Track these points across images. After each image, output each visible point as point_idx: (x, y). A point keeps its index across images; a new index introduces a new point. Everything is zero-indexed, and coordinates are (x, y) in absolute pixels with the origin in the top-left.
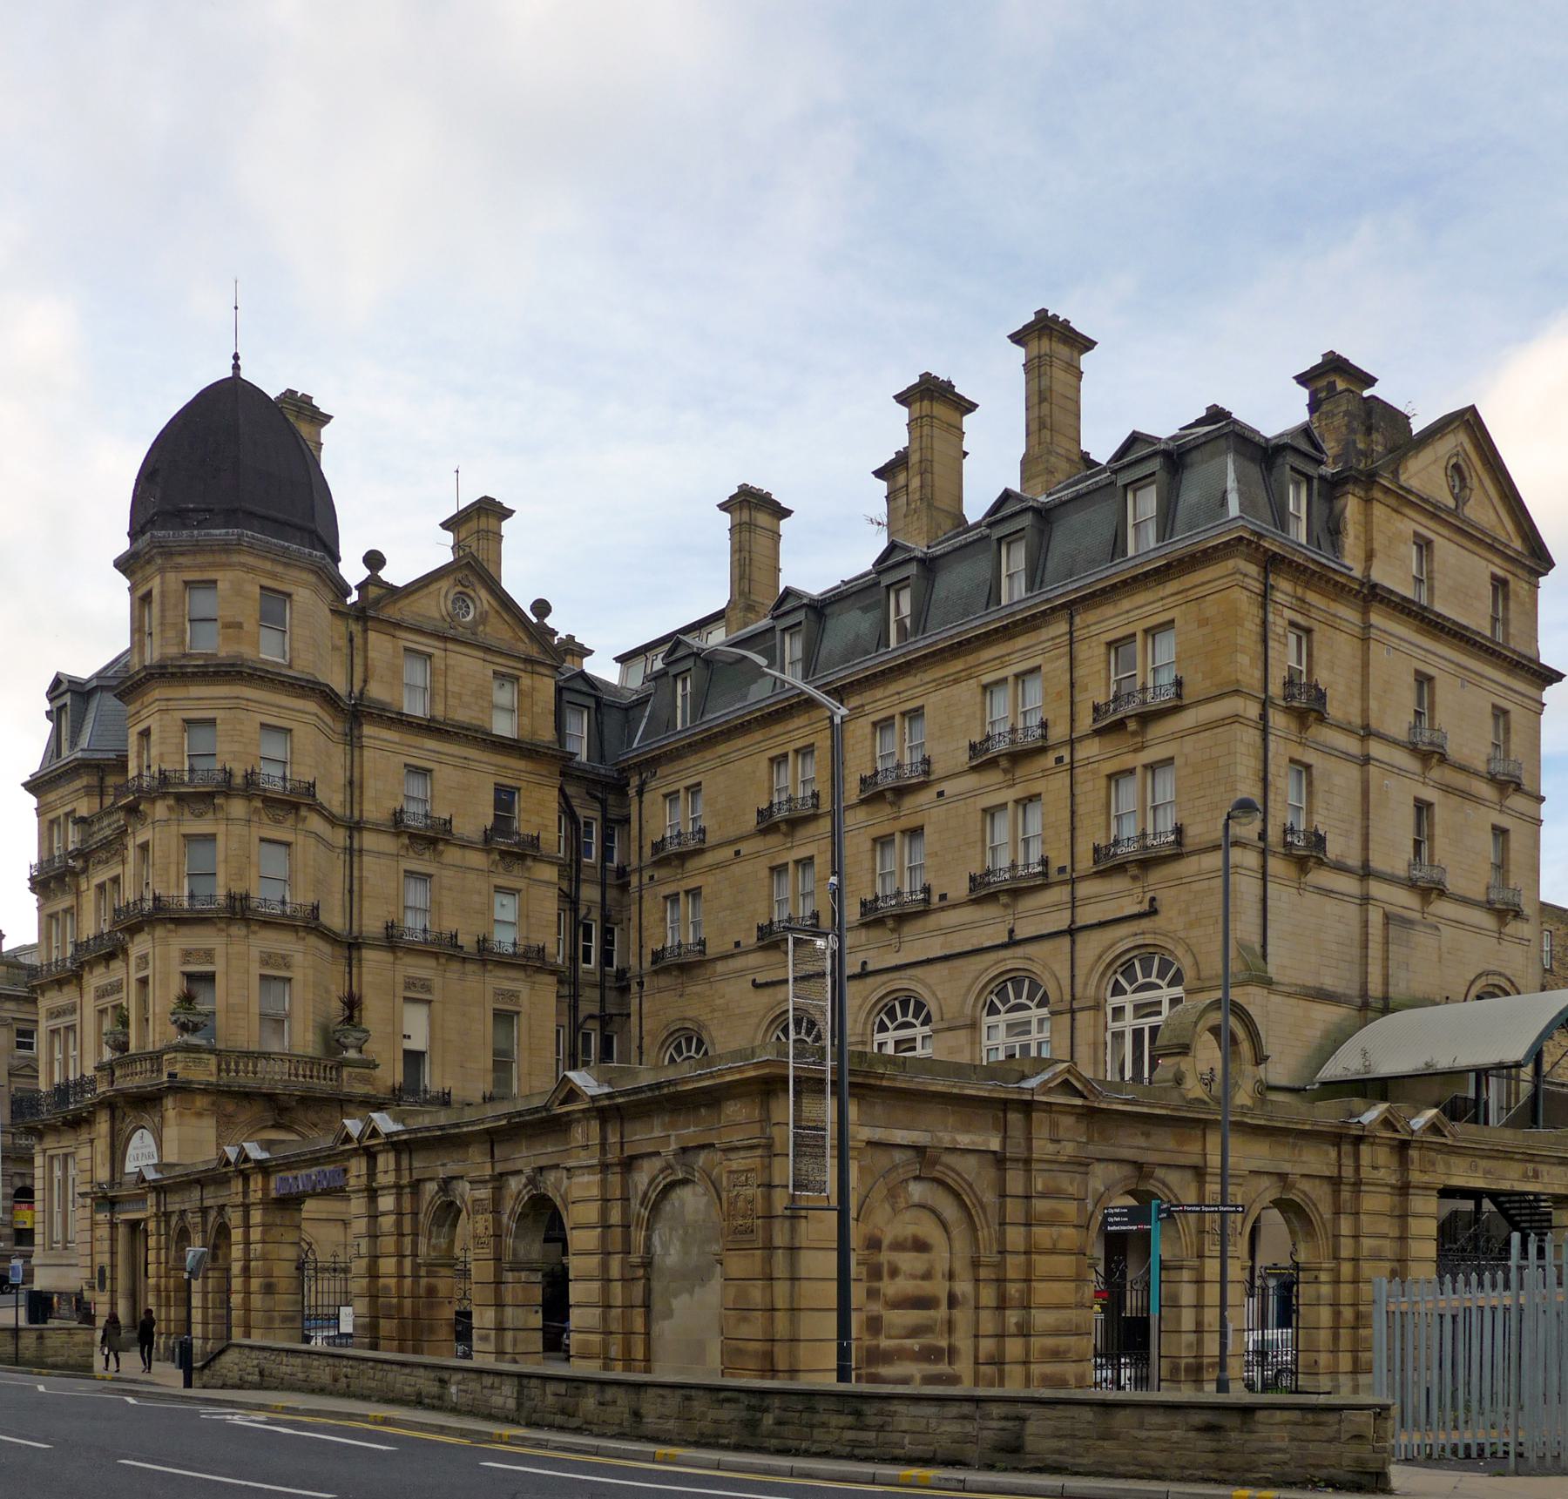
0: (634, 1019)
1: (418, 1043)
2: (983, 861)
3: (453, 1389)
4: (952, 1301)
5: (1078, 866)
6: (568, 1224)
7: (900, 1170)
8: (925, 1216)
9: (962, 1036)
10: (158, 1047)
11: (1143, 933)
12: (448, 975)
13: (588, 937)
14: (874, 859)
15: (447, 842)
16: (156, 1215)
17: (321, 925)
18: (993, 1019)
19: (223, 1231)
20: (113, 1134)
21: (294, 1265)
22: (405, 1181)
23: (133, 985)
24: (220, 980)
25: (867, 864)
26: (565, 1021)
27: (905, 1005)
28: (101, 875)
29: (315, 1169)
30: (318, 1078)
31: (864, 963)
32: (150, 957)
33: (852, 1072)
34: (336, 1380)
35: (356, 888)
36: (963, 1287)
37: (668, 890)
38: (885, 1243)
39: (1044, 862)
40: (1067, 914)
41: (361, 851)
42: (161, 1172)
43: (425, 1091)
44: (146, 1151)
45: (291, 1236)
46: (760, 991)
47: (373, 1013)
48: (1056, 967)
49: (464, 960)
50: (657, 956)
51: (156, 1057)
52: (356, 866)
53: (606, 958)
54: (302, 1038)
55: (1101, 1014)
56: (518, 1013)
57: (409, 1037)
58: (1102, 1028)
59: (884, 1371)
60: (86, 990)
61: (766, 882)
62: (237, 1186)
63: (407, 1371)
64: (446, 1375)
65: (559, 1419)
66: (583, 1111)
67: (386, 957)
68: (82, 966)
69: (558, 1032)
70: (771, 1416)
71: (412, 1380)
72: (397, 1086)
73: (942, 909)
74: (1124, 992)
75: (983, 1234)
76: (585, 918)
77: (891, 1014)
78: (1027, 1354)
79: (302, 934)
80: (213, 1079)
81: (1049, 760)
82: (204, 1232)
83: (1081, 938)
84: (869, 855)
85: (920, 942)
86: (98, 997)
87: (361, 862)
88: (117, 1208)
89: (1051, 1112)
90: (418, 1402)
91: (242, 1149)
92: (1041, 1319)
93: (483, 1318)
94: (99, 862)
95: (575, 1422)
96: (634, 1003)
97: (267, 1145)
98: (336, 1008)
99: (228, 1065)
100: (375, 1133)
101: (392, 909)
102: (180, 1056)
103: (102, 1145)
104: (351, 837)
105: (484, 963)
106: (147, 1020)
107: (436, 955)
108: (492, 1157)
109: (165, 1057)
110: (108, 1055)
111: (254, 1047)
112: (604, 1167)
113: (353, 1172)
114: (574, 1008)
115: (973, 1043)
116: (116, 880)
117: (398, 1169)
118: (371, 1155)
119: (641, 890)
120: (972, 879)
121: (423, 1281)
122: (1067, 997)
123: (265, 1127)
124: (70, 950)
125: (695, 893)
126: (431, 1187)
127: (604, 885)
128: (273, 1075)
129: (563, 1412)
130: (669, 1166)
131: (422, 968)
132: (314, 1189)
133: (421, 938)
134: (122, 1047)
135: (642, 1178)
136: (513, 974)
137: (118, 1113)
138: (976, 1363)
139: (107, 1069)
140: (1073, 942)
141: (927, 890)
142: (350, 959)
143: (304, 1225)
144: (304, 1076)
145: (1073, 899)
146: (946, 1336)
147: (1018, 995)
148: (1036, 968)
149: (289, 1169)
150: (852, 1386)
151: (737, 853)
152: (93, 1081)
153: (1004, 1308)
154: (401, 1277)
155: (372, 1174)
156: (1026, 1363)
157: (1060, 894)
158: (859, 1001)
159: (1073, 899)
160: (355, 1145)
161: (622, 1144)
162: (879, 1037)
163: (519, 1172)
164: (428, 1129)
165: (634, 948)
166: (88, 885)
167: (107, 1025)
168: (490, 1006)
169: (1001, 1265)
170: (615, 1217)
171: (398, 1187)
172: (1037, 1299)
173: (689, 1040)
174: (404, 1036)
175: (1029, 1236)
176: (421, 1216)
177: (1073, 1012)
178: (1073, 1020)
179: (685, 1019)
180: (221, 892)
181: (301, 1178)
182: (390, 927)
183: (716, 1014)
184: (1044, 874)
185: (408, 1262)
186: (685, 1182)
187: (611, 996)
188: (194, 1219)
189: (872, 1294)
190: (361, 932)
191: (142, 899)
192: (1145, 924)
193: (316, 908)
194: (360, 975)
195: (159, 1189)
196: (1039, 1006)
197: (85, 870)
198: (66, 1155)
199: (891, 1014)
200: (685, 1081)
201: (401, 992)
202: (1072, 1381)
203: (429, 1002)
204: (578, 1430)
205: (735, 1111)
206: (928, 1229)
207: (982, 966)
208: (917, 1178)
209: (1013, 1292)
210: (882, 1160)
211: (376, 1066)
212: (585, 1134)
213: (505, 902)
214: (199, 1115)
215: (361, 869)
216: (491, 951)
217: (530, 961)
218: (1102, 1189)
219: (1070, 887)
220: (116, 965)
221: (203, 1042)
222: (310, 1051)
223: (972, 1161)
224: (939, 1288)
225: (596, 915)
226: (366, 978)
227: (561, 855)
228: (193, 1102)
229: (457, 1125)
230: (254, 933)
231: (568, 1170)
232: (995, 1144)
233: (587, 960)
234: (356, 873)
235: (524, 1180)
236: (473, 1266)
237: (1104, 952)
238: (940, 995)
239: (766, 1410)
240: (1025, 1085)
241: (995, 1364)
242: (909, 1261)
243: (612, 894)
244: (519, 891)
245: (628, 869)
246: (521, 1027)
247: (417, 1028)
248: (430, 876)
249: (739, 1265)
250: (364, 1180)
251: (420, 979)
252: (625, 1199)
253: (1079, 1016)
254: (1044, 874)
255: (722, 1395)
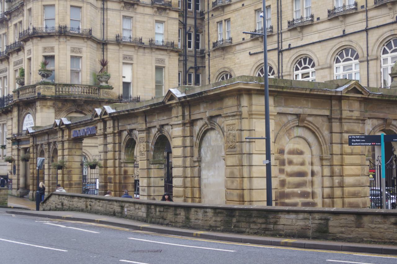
0: (207, 68)
1: (127, 80)
2: (333, 5)
3: (126, 210)
4: (313, 174)
5: (368, 5)
6: (172, 146)
7: (291, 123)
8: (301, 141)
9: (327, 71)
10: (35, 83)
11: (394, 30)
12: (139, 54)
13: (190, 38)
14: (293, 5)
15: (137, 4)
16: (33, 146)
17: (92, 37)
18: (338, 64)
19: (56, 151)
20: (19, 116)
21: (80, 163)
22: (116, 131)
23: (26, 61)
24: (56, 58)
25: (290, 8)
26: (182, 69)
27: (305, 60)
28: (16, 21)
29: (86, 127)
30: (92, 93)
31: (290, 45)
32: (32, 50)
33: (270, 86)
34: (87, 207)
35: (105, 22)
36: (317, 168)
37: (218, 19)
38: (286, 151)
39: (356, 4)
40: (365, 23)
41: (107, 9)
42: (35, 130)
43: (131, 97)
44: (30, 122)
45: (78, 152)
46: (252, 56)
47: (112, 67)
49: (144, 48)
50: (215, 44)
51: (34, 86)
52: (105, 15)
53: (197, 46)
54: (86, 78)
55: (379, 61)
56: (164, 67)
57: (125, 77)
58: (379, 67)
59: (287, 201)
60: (10, 63)
61: (254, 15)
62: (60, 134)
63: (110, 203)
64: (123, 204)
65: (161, 220)
66: (176, 103)
67: (116, 48)
68: (9, 54)
69: (179, 74)
70: (235, 219)
71: (112, 206)
72: (120, 95)
73: (318, 23)
74: (387, 53)
75: (324, 147)
76: (189, 31)
77: (300, 64)
78: (343, 194)
79: (85, 40)
80: (54, 94)
82: (49, 152)
83: (370, 33)
84: (291, 4)
85: (311, 36)
86: (15, 65)
87: (107, 13)
88: (20, 143)
89: (349, 100)
90: (114, 214)
91: (61, 120)
92: (348, 180)
93: (143, 183)
94: (15, 16)
95: (166, 222)
96: (207, 62)
97: (70, 119)
98: (99, 67)
99: (59, 89)
100: (106, 113)
101: (118, 30)
102: (42, 86)
103: (15, 120)
104: (103, 4)
105: (151, 48)
106: (31, 73)
107: (134, 47)
108: (146, 121)
109: (37, 87)
110: (18, 86)
111: (68, 82)
112: (184, 124)
113: (99, 128)
114: (185, 65)
115: (330, 74)
116: (20, 22)
117: (114, 127)
118: (104, 122)
119: (209, 20)
120: (329, 12)
121: (123, 169)
122: (366, 55)
123: (72, 112)
124: (5, 48)
125: (228, 20)
126: (125, 134)
127: (195, 19)
128: (76, 92)
129: (163, 218)
130: (206, 123)
131: (129, 52)
132: (86, 134)
133: (129, 40)
134: (22, 84)
135: (197, 128)
136: (162, 52)
137: (21, 108)
138: (323, 198)
139: (17, 92)
140: (367, 34)
141: (312, 16)
142: (103, 49)
143: (83, 148)
144: (87, 93)
145: (367, 17)
146: (311, 187)
147: (347, 55)
148: (354, 45)
149: (77, 127)
150: (274, 207)
151: (243, 5)
152: (12, 97)
153: (333, 176)
154: (115, 167)
155: (105, 129)
156: (343, 198)
157: (362, 16)
158: (288, 59)
159: (367, 17)
160: (99, 118)
161: (190, 115)
162: (296, 73)
163: (155, 127)
164: (123, 111)
165: (207, 42)
166: (11, 25)
167: (18, 75)
168: (154, 65)
169: (331, 160)
170: (188, 143)
171: (114, 134)
172: (346, 173)
173: (227, 76)
174: (123, 77)
175: (342, 148)
176: (122, 144)
177: (368, 61)
178: (368, 64)
179: (225, 68)
180: (57, 26)
181: (81, 131)
182: (118, 37)
183: (236, 66)
184: (356, 9)
185: (117, 162)
186: (212, 129)
187: (199, 60)
188: (45, 147)
189: (282, 171)
190: (107, 39)
191: (29, 29)
193: (91, 31)
194: (107, 54)
195: (34, 136)
196: (355, 59)
197: (10, 19)
198: (3, 124)
199: (300, 64)
200: (209, 91)
201: (122, 61)
202: (361, 205)
203: (132, 64)
204: (167, 225)
205: (230, 102)
206: (301, 146)
207: (333, 44)
208: (298, 126)
209: (336, 169)
210: (285, 119)
211: (112, 88)
212: (177, 112)
213: (159, 26)
214: (49, 108)
215: (107, 16)
216: (154, 44)
217: (168, 48)
218: (371, 129)
219: (365, 14)
220: (21, 53)
221: (50, 81)
222: (89, 83)
223: (320, 119)
224: (307, 169)
225: (193, 30)
226: (109, 55)
227: (180, 8)
228: (47, 103)
229: (133, 110)
230: (69, 40)
231: (171, 125)
232: (327, 113)
233: (190, 47)
234: (105, 17)
235: (157, 130)
236: (140, 163)
237: (379, 38)
238: (318, 56)
239: (234, 216)
240: (338, 90)
241: (330, 198)
242: (296, 159)
243: (198, 21)
244: (164, 22)
245: (204, 12)
246: (165, 72)
247: (127, 74)
248: (132, 17)
249: (232, 160)
250: (102, 131)
251: (128, 55)
252: (191, 136)
253: (370, 62)
254: (356, 9)
255: (218, 211)
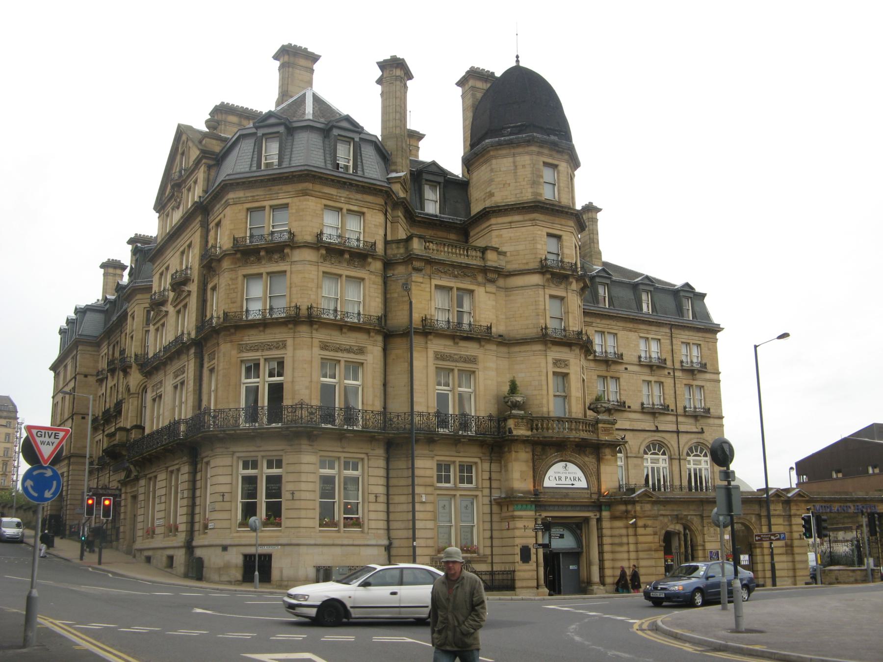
48: (672, 443)
81: (666, 372)
83: (680, 435)
140: (678, 436)
192: (699, 436)
